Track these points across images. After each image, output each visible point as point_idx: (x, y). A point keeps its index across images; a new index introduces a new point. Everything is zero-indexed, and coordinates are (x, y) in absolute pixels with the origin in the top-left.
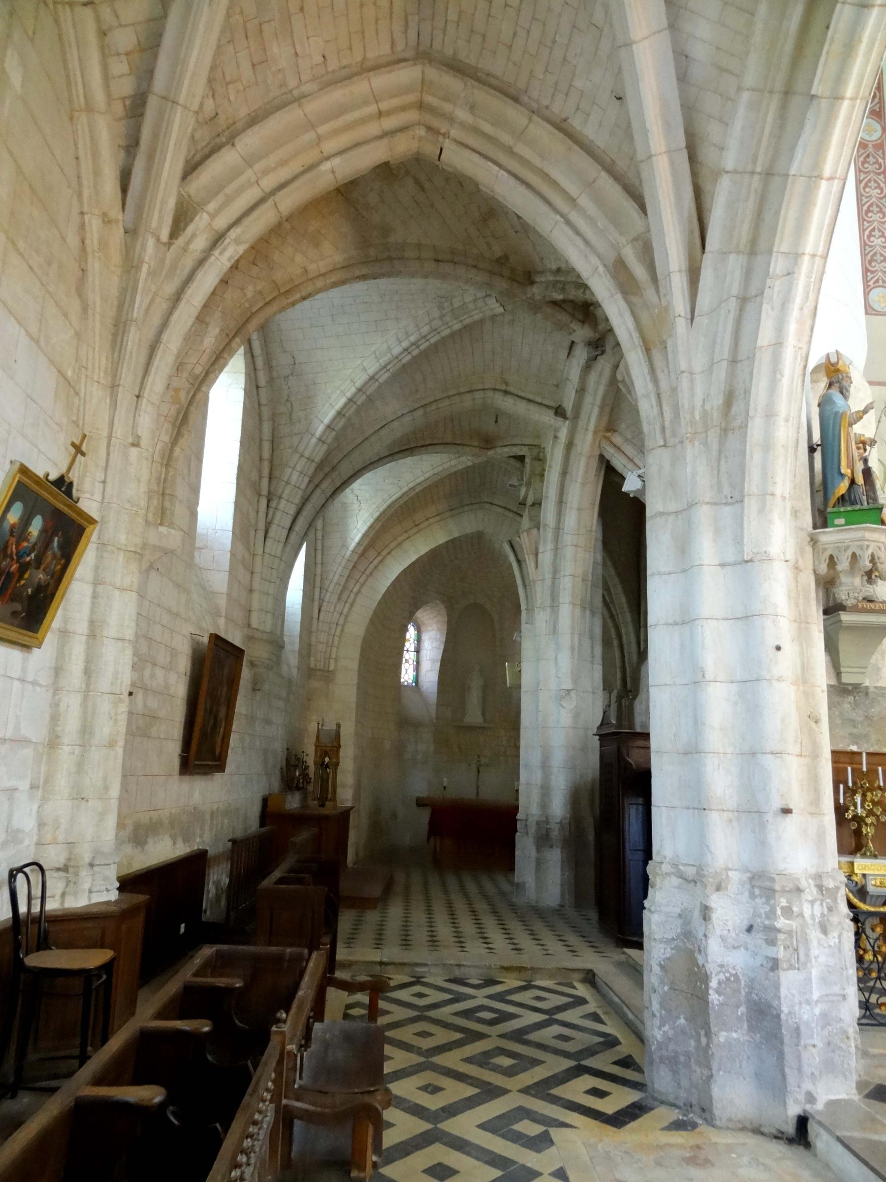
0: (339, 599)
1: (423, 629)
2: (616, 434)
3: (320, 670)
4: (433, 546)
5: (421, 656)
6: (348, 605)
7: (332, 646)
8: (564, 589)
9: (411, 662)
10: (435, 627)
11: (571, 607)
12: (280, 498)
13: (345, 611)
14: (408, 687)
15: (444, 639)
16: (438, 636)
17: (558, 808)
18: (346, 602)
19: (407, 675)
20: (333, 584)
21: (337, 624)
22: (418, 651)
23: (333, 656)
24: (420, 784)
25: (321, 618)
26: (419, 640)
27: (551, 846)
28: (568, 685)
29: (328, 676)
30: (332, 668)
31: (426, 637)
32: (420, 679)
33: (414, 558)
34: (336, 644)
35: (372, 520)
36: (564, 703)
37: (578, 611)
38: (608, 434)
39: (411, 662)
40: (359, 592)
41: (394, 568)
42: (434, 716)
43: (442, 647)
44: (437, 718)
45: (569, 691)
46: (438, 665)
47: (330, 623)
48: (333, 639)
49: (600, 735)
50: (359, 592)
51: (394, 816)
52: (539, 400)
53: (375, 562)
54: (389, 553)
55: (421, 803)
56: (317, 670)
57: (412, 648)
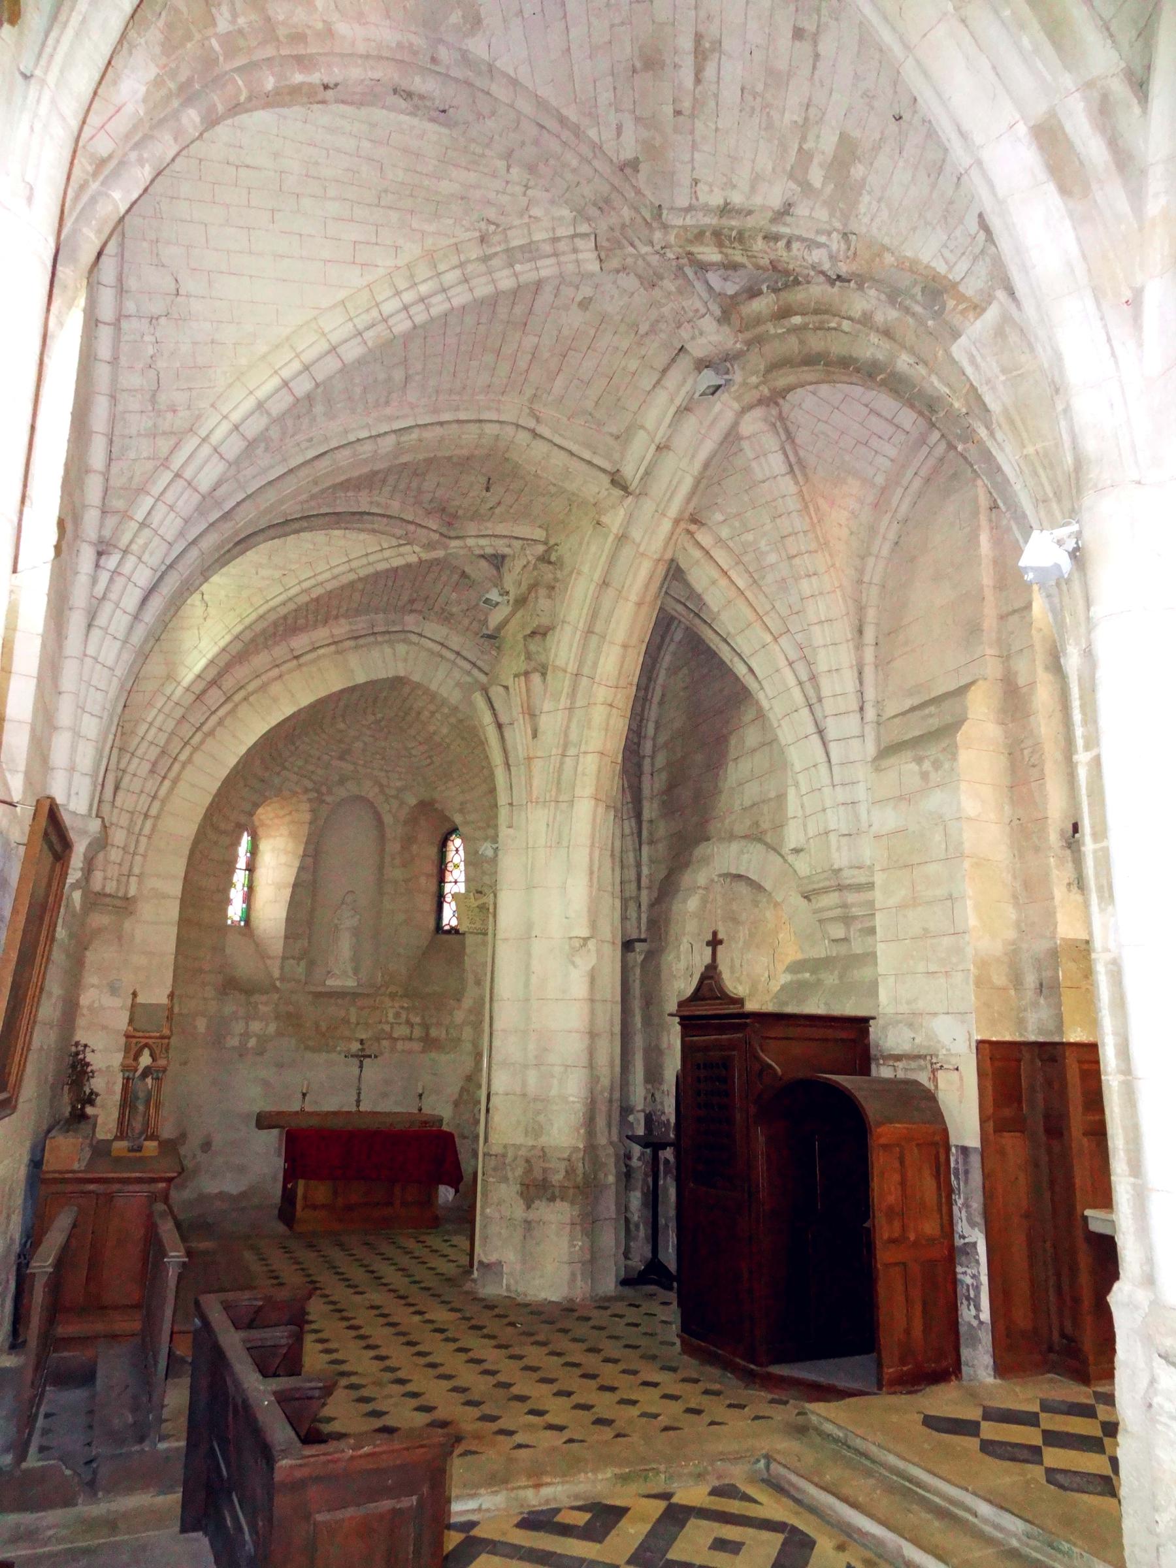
0: (152, 771)
1: (260, 832)
2: (703, 529)
3: (110, 895)
5: (266, 879)
6: (167, 783)
7: (134, 854)
8: (584, 774)
10: (284, 830)
11: (593, 802)
12: (126, 552)
13: (163, 792)
14: (235, 925)
15: (301, 852)
16: (291, 846)
17: (563, 1132)
18: (164, 778)
19: (235, 911)
20: (145, 744)
21: (146, 816)
22: (251, 868)
23: (136, 870)
24: (253, 1091)
25: (118, 803)
26: (254, 851)
27: (552, 1199)
28: (584, 932)
29: (125, 906)
30: (132, 892)
31: (265, 846)
32: (253, 915)
33: (289, 711)
34: (141, 850)
35: (228, 638)
36: (577, 960)
37: (601, 810)
38: (693, 527)
40: (189, 760)
41: (253, 726)
42: (276, 973)
43: (297, 864)
44: (282, 979)
45: (586, 939)
46: (288, 892)
47: (132, 813)
48: (137, 841)
49: (683, 1018)
50: (189, 760)
51: (206, 1146)
52: (587, 455)
53: (221, 713)
54: (245, 699)
55: (264, 1121)
56: (106, 895)
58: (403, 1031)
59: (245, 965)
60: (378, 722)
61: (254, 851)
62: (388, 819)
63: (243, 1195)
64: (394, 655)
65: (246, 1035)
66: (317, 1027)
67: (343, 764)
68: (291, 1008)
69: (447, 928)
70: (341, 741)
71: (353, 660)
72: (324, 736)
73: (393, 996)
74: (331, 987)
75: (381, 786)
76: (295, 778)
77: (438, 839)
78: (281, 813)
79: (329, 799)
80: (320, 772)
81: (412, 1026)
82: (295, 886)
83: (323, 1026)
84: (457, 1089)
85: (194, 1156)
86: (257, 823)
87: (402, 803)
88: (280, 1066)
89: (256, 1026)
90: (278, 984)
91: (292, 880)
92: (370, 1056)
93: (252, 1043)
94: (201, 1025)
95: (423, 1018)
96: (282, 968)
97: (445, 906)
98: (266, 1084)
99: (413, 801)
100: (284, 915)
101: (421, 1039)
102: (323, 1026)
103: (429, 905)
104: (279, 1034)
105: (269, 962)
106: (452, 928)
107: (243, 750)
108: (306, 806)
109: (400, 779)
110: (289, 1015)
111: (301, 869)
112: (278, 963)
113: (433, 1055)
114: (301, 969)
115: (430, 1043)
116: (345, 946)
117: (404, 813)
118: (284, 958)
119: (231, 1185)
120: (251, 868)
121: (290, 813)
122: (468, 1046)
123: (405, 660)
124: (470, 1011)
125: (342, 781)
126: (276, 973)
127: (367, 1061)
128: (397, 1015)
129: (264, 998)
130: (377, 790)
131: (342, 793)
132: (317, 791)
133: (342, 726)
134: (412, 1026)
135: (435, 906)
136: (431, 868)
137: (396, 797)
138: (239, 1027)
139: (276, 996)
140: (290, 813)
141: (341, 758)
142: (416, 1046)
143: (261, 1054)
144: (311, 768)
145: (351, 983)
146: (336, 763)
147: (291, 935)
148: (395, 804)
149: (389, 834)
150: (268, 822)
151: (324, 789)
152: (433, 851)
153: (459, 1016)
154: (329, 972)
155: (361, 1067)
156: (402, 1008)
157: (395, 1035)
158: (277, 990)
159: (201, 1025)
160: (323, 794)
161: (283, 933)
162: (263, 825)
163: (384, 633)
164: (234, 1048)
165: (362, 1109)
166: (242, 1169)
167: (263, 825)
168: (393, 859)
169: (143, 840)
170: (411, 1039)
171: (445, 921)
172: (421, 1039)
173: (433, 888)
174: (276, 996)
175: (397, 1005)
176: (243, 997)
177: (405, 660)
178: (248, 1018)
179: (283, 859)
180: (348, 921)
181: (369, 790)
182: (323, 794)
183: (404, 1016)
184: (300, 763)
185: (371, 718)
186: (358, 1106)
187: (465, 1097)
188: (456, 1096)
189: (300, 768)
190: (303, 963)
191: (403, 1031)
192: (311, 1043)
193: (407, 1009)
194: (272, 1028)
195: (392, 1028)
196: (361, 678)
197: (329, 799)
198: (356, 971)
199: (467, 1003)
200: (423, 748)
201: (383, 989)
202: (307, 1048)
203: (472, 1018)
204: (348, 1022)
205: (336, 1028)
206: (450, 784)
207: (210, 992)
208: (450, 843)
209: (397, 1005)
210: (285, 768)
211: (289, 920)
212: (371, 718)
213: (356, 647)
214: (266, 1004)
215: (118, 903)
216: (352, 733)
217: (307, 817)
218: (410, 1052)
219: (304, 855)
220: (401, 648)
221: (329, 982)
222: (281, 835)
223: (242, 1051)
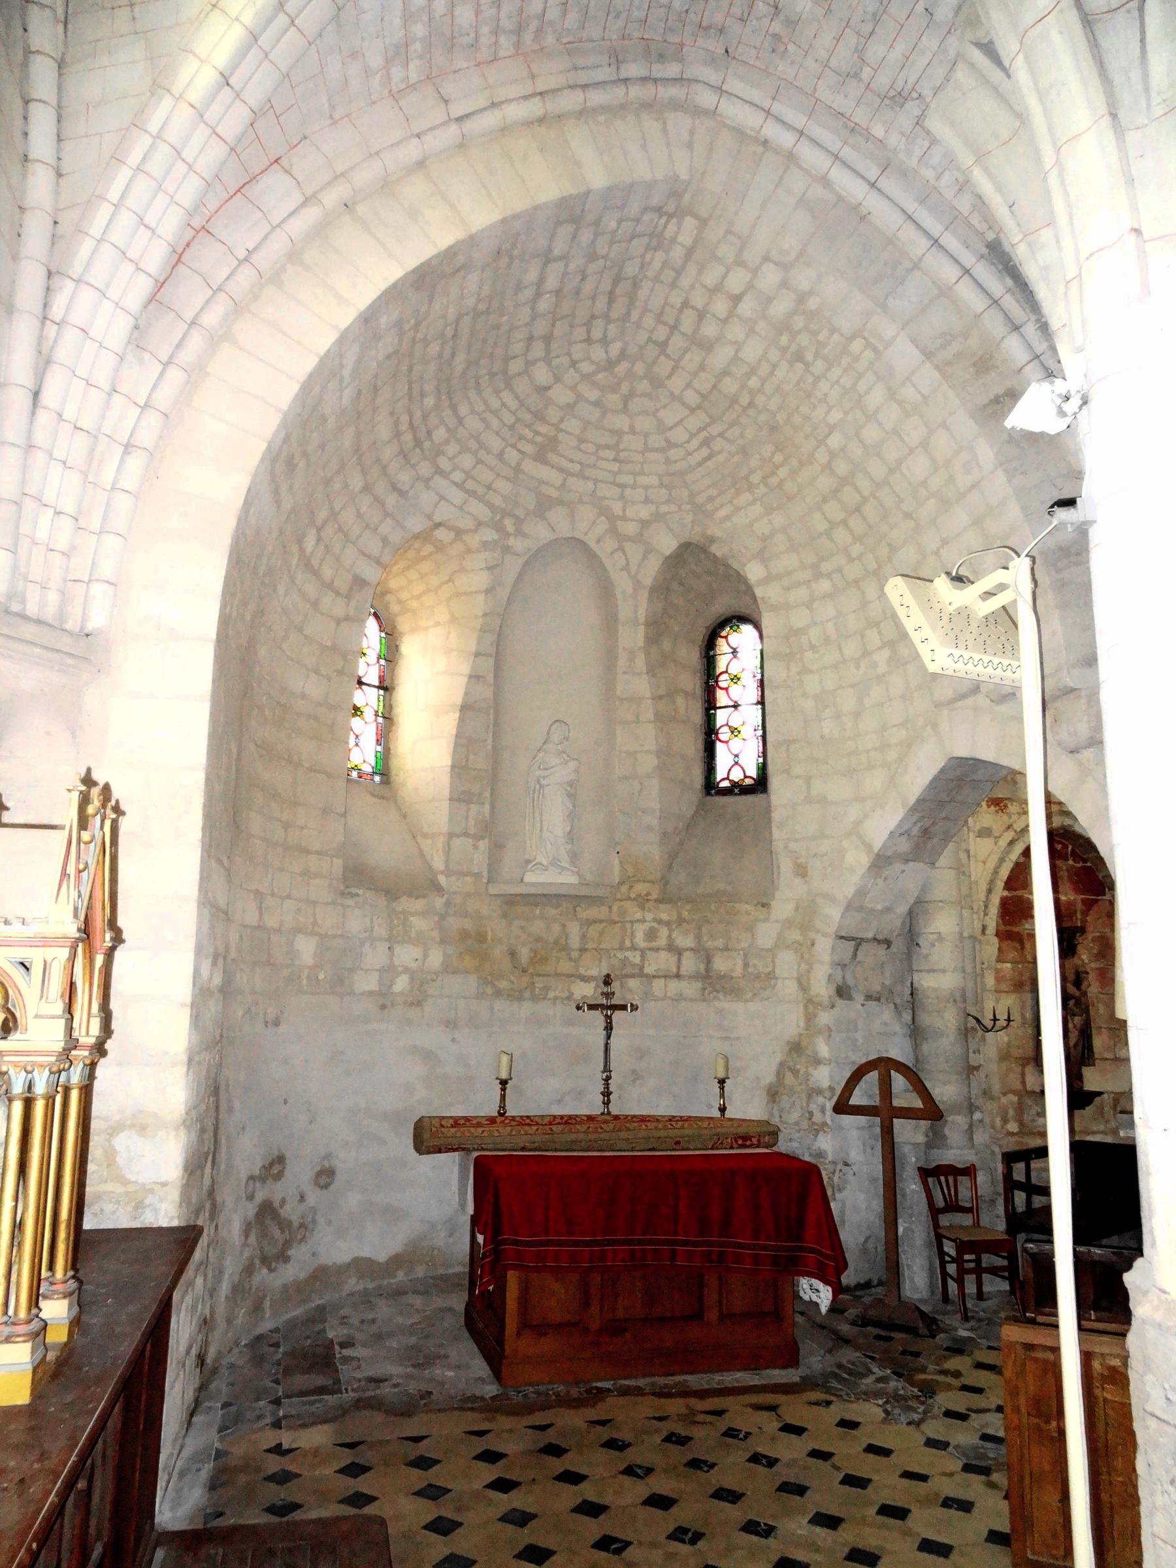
1: (403, 624)
3: (39, 622)
4: (519, 205)
9: (369, 714)
19: (363, 753)
21: (128, 448)
25: (50, 397)
31: (411, 648)
32: (395, 763)
33: (444, 238)
39: (369, 714)
43: (465, 668)
44: (448, 873)
46: (450, 723)
51: (325, 1176)
55: (430, 1137)
57: (372, 677)
58: (661, 961)
59: (385, 848)
60: (610, 364)
61: (391, 655)
62: (622, 584)
63: (397, 1261)
64: (664, 130)
65: (389, 971)
66: (512, 954)
67: (543, 472)
68: (467, 924)
69: (725, 784)
70: (539, 416)
71: (580, 140)
72: (507, 397)
73: (642, 901)
74: (533, 884)
75: (612, 519)
76: (456, 496)
77: (700, 635)
78: (434, 581)
79: (517, 544)
80: (503, 486)
81: (679, 952)
82: (466, 708)
83: (524, 954)
84: (774, 1067)
85: (302, 1198)
86: (395, 608)
87: (649, 550)
88: (451, 1024)
89: (407, 955)
90: (442, 879)
91: (459, 700)
92: (623, 1007)
93: (401, 984)
94: (306, 948)
95: (698, 937)
96: (448, 849)
97: (719, 747)
98: (429, 1056)
99: (667, 544)
100: (447, 761)
101: (695, 977)
102: (524, 954)
103: (693, 747)
104: (448, 968)
105: (426, 845)
106: (735, 785)
107: (346, 317)
108: (480, 560)
109: (647, 501)
110: (464, 935)
111: (475, 677)
112: (440, 842)
113: (725, 1003)
114: (480, 859)
115: (712, 982)
116: (555, 815)
117: (651, 570)
118: (451, 835)
119: (379, 1244)
120: (386, 687)
121: (451, 580)
122: (788, 988)
123: (690, 145)
124: (788, 924)
125: (542, 508)
126: (438, 863)
127: (618, 1016)
128: (651, 935)
129: (419, 905)
130: (603, 525)
131: (540, 533)
132: (499, 528)
133: (542, 375)
134: (679, 952)
135: (700, 745)
136: (692, 682)
137: (638, 539)
138: (375, 956)
139: (439, 902)
140: (451, 580)
141: (540, 457)
142: (691, 989)
143: (419, 1004)
144: (486, 476)
145: (565, 879)
146: (529, 466)
147: (460, 797)
148: (634, 552)
149: (624, 611)
150: (414, 604)
151: (509, 524)
152: (692, 656)
153: (766, 934)
154: (528, 862)
155: (609, 1028)
156: (660, 922)
157: (648, 970)
158: (438, 889)
159: (306, 948)
160: (508, 535)
161: (446, 793)
162: (405, 610)
163: (644, 80)
164: (371, 993)
165: (615, 1109)
166: (393, 1214)
167: (405, 610)
168: (632, 660)
169: (123, 503)
170: (678, 976)
171: (720, 773)
172: (695, 977)
173: (698, 717)
174: (439, 902)
175: (649, 916)
176: (382, 902)
177: (690, 145)
178: (392, 941)
179: (441, 663)
180: (561, 773)
181: (587, 525)
182: (508, 535)
183: (664, 932)
184: (467, 461)
185: (598, 353)
186: (607, 1103)
187: (789, 1079)
188: (769, 1078)
189: (468, 475)
190: (483, 844)
191: (661, 961)
192: (503, 984)
193: (668, 924)
194: (435, 959)
195: (643, 956)
196: (597, 178)
197: (517, 544)
198: (574, 857)
199: (783, 908)
200: (701, 418)
201: (624, 889)
202: (498, 993)
203: (795, 935)
204: (565, 948)
205: (544, 960)
206: (746, 497)
207: (320, 890)
208: (721, 642)
209: (649, 916)
210: (439, 472)
211: (459, 768)
212: (598, 353)
213: (583, 113)
214: (423, 914)
215: (65, 643)
216: (562, 395)
217: (481, 580)
218: (680, 998)
219: (477, 655)
220: (680, 123)
221: (530, 878)
222: (437, 624)
223: (384, 1001)
